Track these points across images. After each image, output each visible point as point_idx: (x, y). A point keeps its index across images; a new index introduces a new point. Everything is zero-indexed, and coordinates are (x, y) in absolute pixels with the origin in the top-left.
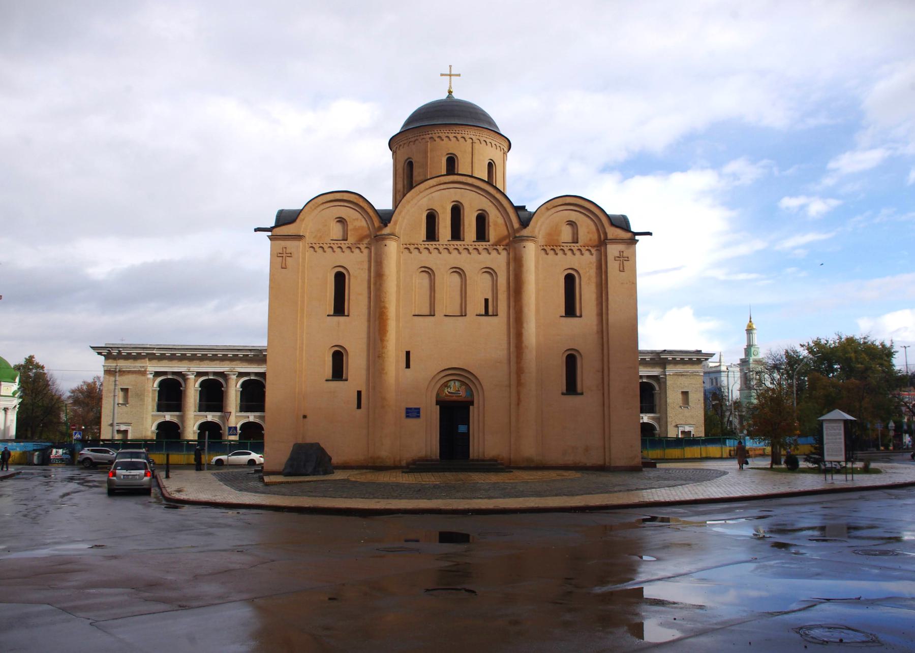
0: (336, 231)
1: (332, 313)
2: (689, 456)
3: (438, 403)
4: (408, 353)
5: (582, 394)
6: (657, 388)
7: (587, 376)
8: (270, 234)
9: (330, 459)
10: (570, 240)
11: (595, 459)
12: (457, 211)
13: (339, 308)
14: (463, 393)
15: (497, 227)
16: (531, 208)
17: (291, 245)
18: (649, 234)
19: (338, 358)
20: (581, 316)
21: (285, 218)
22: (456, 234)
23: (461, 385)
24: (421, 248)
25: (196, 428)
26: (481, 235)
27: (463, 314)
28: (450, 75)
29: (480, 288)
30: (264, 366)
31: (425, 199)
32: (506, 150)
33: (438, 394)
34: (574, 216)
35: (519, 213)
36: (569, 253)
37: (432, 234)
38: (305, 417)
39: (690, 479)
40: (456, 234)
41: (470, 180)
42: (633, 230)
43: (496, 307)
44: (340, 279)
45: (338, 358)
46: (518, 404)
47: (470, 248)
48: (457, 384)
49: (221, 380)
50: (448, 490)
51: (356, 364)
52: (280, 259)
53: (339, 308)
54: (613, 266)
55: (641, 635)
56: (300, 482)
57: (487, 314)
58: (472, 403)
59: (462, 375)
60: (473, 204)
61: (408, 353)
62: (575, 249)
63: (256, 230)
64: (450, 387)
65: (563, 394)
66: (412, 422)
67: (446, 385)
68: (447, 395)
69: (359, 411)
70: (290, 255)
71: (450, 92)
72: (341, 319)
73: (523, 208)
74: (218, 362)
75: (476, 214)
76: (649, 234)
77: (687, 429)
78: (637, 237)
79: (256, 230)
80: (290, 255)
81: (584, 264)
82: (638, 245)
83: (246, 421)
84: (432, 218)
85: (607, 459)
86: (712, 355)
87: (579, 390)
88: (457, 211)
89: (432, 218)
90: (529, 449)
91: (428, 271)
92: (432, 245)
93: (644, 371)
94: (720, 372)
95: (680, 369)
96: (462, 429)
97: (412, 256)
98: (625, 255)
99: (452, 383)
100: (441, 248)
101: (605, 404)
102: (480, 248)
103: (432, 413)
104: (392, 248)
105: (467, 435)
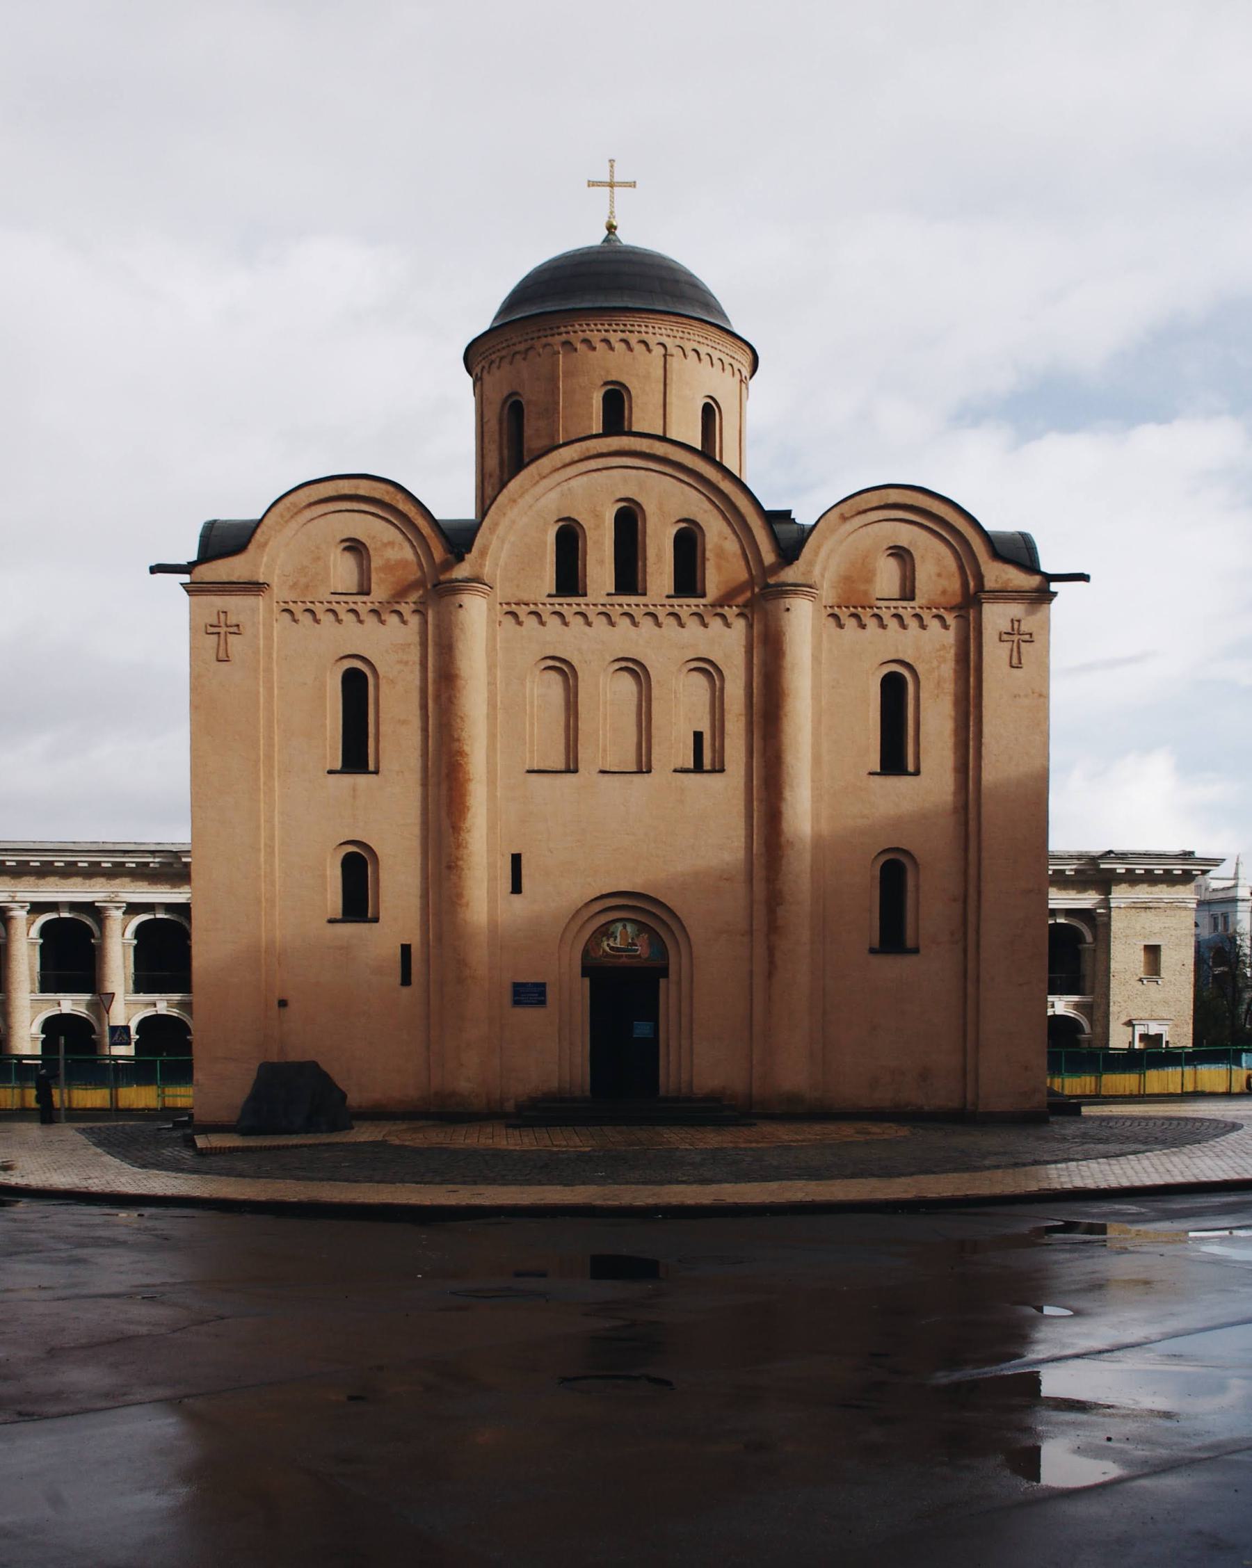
0: (343, 571)
1: (338, 765)
2: (1156, 1091)
3: (586, 971)
4: (516, 860)
5: (916, 951)
6: (1089, 938)
7: (930, 909)
8: (186, 578)
9: (344, 1096)
10: (895, 591)
11: (942, 1095)
12: (629, 522)
13: (356, 755)
14: (642, 949)
15: (723, 561)
16: (805, 516)
17: (235, 604)
18: (1084, 577)
19: (357, 870)
20: (917, 773)
21: (222, 541)
22: (629, 578)
23: (640, 932)
24: (545, 611)
25: (36, 1028)
26: (687, 579)
27: (644, 767)
28: (611, 185)
29: (683, 708)
30: (186, 889)
31: (553, 495)
32: (746, 373)
33: (586, 953)
34: (906, 535)
35: (777, 527)
36: (893, 624)
37: (569, 579)
38: (283, 1003)
39: (1157, 1141)
40: (629, 578)
41: (660, 449)
42: (1043, 569)
43: (719, 752)
44: (356, 687)
45: (357, 870)
46: (770, 975)
47: (661, 613)
48: (629, 928)
49: (89, 921)
50: (612, 1166)
51: (399, 884)
52: (215, 638)
53: (356, 755)
54: (995, 654)
55: (1035, 1474)
56: (278, 1148)
57: (698, 768)
58: (664, 972)
59: (641, 909)
60: (667, 503)
61: (516, 860)
62: (907, 615)
63: (155, 569)
64: (612, 935)
65: (872, 951)
66: (528, 1015)
67: (605, 931)
68: (606, 955)
69: (405, 991)
70: (237, 629)
71: (611, 228)
72: (361, 780)
73: (785, 516)
74: (78, 880)
75: (673, 530)
76: (1084, 577)
77: (1154, 1029)
78: (1054, 586)
79: (155, 569)
80: (237, 629)
81: (929, 647)
82: (1055, 602)
83: (150, 1012)
84: (569, 540)
85: (970, 1097)
86: (1216, 862)
87: (910, 943)
88: (629, 522)
89: (569, 540)
90: (794, 1073)
91: (563, 669)
92: (570, 605)
93: (1059, 899)
94: (1234, 900)
95: (1143, 893)
96: (641, 1029)
97: (523, 630)
98: (1024, 628)
99: (619, 926)
100: (591, 612)
101: (968, 977)
102: (684, 613)
103: (573, 995)
104: (475, 613)
105: (651, 1047)
